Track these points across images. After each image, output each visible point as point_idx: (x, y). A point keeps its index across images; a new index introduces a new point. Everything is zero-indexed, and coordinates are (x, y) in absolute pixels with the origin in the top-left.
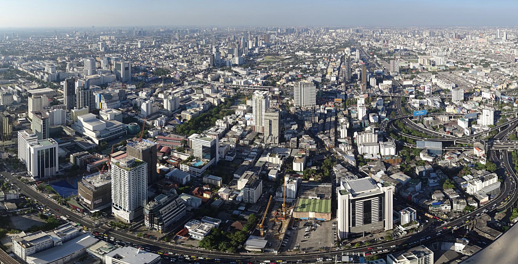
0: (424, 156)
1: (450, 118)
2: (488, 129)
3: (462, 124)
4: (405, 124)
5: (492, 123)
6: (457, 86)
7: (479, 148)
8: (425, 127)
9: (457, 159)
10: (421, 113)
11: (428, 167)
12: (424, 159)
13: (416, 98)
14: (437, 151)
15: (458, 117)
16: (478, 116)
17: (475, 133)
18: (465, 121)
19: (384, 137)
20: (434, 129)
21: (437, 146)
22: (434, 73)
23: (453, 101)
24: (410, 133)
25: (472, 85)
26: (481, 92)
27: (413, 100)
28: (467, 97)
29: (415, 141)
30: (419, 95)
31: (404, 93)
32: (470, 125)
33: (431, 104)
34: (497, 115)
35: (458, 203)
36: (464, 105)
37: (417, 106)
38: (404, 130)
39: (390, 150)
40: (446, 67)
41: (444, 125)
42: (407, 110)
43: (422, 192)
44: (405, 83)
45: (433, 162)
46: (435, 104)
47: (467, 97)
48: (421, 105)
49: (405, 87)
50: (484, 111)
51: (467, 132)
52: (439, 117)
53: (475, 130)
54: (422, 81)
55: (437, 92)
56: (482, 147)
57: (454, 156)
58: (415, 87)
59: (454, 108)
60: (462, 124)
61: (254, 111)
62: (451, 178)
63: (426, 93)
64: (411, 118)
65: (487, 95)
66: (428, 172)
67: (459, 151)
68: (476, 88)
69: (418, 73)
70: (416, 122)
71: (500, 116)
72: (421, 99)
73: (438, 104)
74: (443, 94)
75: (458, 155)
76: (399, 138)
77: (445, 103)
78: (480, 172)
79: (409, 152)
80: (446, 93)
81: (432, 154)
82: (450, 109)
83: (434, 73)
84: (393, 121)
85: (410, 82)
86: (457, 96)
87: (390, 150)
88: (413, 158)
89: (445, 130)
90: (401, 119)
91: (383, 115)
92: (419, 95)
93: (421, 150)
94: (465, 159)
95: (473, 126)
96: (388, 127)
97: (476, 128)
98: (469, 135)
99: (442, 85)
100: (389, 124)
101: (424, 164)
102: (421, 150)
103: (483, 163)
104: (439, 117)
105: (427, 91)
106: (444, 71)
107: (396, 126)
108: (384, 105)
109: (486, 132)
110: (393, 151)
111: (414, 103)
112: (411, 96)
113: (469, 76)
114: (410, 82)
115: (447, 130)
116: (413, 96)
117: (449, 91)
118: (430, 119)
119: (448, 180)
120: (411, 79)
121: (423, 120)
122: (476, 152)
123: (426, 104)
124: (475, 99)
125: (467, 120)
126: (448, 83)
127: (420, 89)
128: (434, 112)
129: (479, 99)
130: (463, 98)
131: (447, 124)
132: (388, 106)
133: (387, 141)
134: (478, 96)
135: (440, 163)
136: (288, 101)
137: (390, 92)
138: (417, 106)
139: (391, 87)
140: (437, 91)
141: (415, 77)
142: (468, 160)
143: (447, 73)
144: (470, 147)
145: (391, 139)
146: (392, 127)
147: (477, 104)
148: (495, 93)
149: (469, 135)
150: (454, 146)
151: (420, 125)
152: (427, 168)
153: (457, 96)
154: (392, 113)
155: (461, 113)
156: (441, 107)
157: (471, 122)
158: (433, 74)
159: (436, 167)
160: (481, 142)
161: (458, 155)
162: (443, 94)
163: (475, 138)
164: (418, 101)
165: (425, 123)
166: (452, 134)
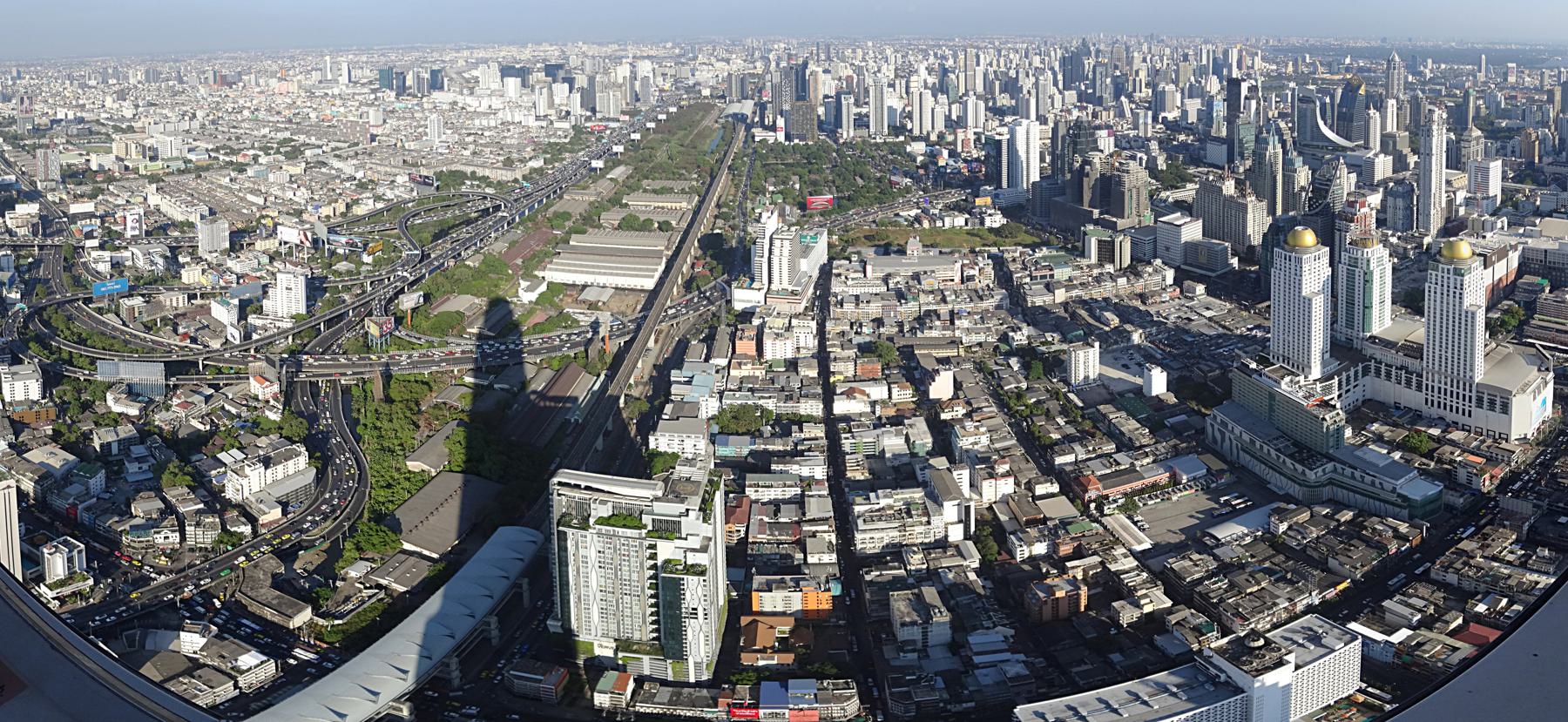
0: (117, 400)
1: (192, 297)
2: (290, 325)
3: (223, 313)
4: (70, 318)
5: (303, 310)
7: (262, 377)
8: (124, 324)
9: (204, 408)
10: (113, 286)
11: (127, 430)
12: (117, 409)
13: (102, 247)
14: (153, 387)
15: (214, 296)
16: (265, 293)
17: (255, 337)
20: (148, 328)
21: (151, 374)
22: (153, 179)
23: (201, 252)
24: (82, 341)
27: (95, 254)
28: (238, 241)
29: (93, 361)
30: (110, 240)
31: (71, 234)
32: (242, 316)
33: (141, 263)
34: (315, 288)
35: (198, 525)
36: (230, 263)
37: (104, 268)
38: (67, 333)
39: (26, 387)
40: (187, 161)
41: (176, 316)
42: (77, 282)
44: (74, 209)
45: (139, 417)
46: (152, 263)
47: (238, 241)
48: (116, 265)
49: (74, 218)
51: (235, 335)
52: (161, 298)
53: (255, 329)
54: (120, 201)
55: (159, 229)
56: (271, 373)
57: (196, 398)
58: (102, 218)
59: (204, 271)
60: (223, 313)
62: (185, 460)
63: (129, 234)
64: (88, 301)
66: (125, 444)
67: (210, 386)
69: (111, 179)
70: (100, 311)
71: (325, 290)
72: (118, 249)
73: (161, 261)
74: (176, 234)
75: (208, 398)
76: (52, 353)
77: (181, 259)
78: (263, 442)
79: (79, 392)
80: (183, 232)
81: (138, 395)
82: (191, 275)
83: (153, 179)
84: (38, 311)
85: (88, 207)
86: (211, 238)
87: (26, 387)
88: (86, 406)
89: (175, 331)
90: (60, 304)
92: (110, 240)
93: (110, 386)
94: (227, 407)
95: (253, 319)
96: (26, 326)
97: (259, 323)
98: (237, 342)
99: (174, 210)
100: (29, 318)
101: (116, 422)
102: (110, 386)
103: (274, 416)
104: (161, 298)
105: (133, 228)
106: (181, 172)
107: (47, 324)
108: (17, 268)
109: (283, 333)
110: (35, 391)
111: (96, 261)
112: (89, 243)
114: (88, 207)
115: (181, 330)
116: (95, 243)
117: (192, 225)
118: (137, 301)
119: (176, 462)
120: (93, 196)
121: (118, 306)
122: (255, 387)
123: (129, 263)
124: (260, 245)
125: (236, 301)
127: (116, 222)
128: (145, 285)
131: (184, 315)
132: (29, 270)
135: (160, 419)
137: (35, 234)
138: (104, 268)
139: (36, 220)
140: (160, 227)
141: (102, 191)
142: (234, 411)
143: (189, 179)
144: (242, 376)
146: (36, 326)
147: (265, 260)
148: (312, 229)
149: (237, 342)
150: (198, 373)
151: (110, 318)
152: (122, 435)
153: (211, 238)
154: (39, 288)
155: (222, 283)
156: (167, 269)
157: (244, 309)
158: (150, 183)
159: (145, 432)
160: (268, 360)
161: (208, 398)
162: (176, 234)
163: (257, 350)
164: (107, 255)
165: (124, 315)
166: (194, 340)
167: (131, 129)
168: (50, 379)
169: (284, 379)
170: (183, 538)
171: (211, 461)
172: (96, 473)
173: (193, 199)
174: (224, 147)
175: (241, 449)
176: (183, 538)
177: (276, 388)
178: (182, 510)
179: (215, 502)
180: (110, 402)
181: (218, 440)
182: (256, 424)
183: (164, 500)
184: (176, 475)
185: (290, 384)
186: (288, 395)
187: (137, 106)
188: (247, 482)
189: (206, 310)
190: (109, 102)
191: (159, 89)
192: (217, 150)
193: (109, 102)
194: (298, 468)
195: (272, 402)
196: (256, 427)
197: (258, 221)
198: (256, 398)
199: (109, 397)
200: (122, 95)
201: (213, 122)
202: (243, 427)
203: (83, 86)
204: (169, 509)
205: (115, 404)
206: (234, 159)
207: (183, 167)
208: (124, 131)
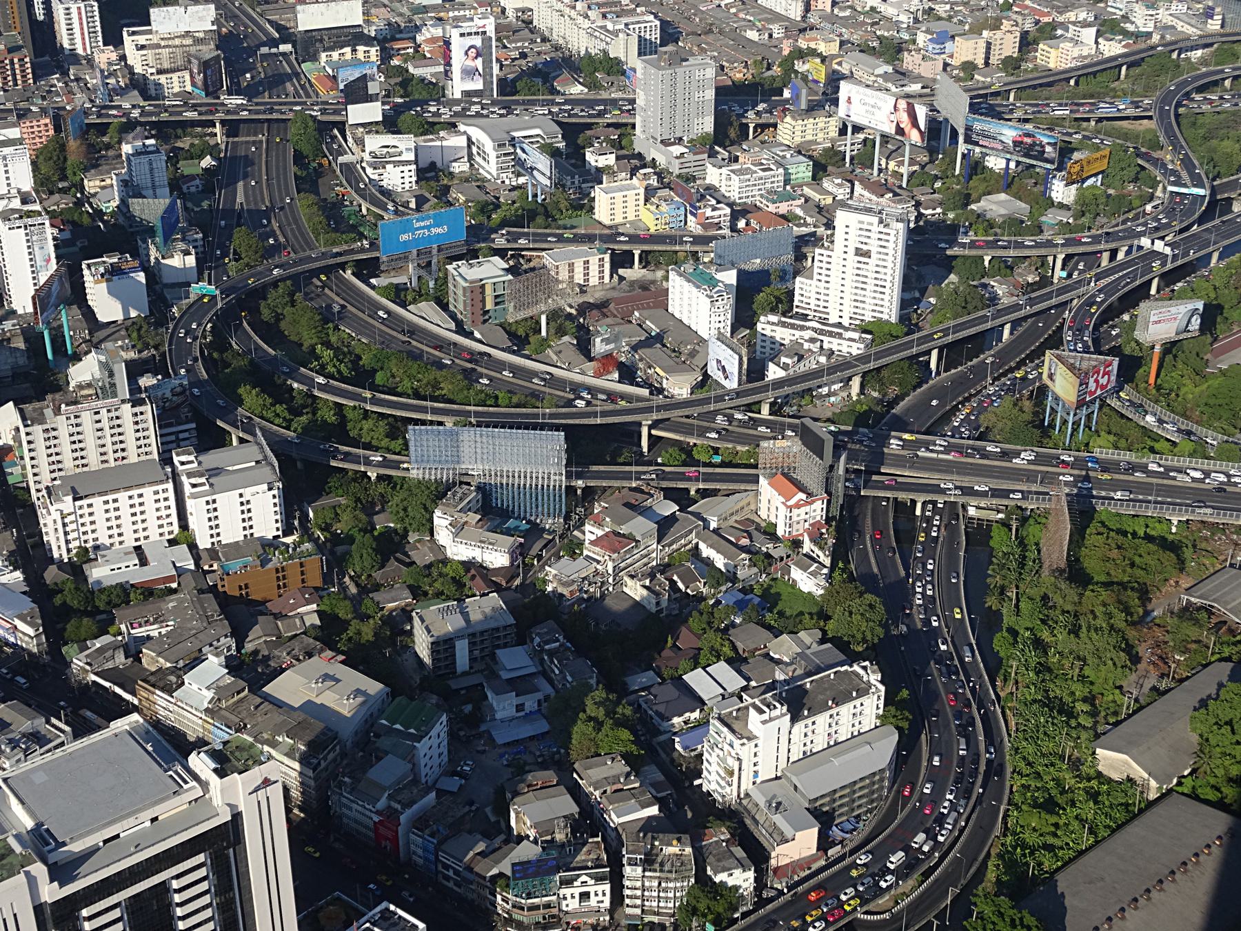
2: (856, 349)
4: (327, 317)
5: (890, 313)
6: (669, 34)
7: (790, 480)
8: (460, 329)
9: (656, 552)
10: (430, 228)
11: (484, 606)
12: (459, 551)
13: (390, 124)
14: (538, 493)
15: (674, 260)
16: (800, 257)
17: (774, 372)
18: (712, 283)
19: (197, 416)
20: (519, 339)
21: (530, 460)
23: (641, 141)
24: (362, 377)
25: (778, 32)
26: (834, 80)
27: (374, 143)
30: (413, 106)
32: (744, 317)
33: (491, 167)
36: (714, 175)
37: (399, 179)
38: (327, 354)
42: (336, 218)
43: (454, 784)
45: (509, 573)
46: (521, 167)
48: (431, 173)
50: (842, 218)
51: (726, 364)
52: (547, 259)
53: (775, 350)
56: (810, 469)
57: (640, 526)
58: (387, 41)
62: (616, 687)
63: (458, 87)
64: (368, 269)
65: (870, 106)
67: (670, 494)
68: (801, 54)
70: (399, 294)
72: (429, 128)
73: (543, 163)
74: (577, 90)
75: (665, 525)
76: (296, 412)
77: (590, 157)
79: (369, 509)
80: (593, 85)
81: (505, 514)
84: (244, 303)
86: (668, 104)
88: (390, 546)
89: (584, 347)
90: (300, 281)
91: (176, 261)
92: (413, 106)
93: (440, 492)
94: (706, 551)
95: (768, 326)
96: (219, 343)
97: (784, 335)
100: (225, 322)
101: (459, 584)
102: (440, 492)
104: (547, 259)
105: (469, 73)
107: (271, 332)
109: (840, 368)
111: (379, 162)
112: (359, 113)
117: (615, 68)
118: (491, 269)
119: (600, 694)
122: (771, 504)
123: (460, 167)
129: (819, 131)
131: (601, 307)
133: (220, 440)
134: (813, 108)
135: (557, 576)
138: (399, 179)
140: (535, 72)
142: (720, 562)
144: (743, 472)
145: (249, 428)
146: (248, 341)
149: (732, 384)
150: (640, 460)
151: (425, 315)
152: (475, 616)
153: (668, 104)
154: (240, 238)
156: (559, 185)
159: (531, 608)
161: (665, 525)
162: (577, 90)
163: (776, 409)
164: (405, 144)
166: (628, 374)
169: (839, 488)
170: (618, 897)
171: (669, 691)
175: (737, 662)
176: (618, 897)
177: (817, 510)
178: (615, 819)
179: (686, 807)
180: (443, 536)
181: (686, 640)
182: (770, 598)
183: (576, 792)
184: (599, 725)
185: (852, 503)
186: (844, 526)
188: (754, 754)
189: (656, 297)
194: (859, 719)
196: (771, 607)
197: (788, 68)
198: (770, 532)
199: (441, 521)
202: (740, 606)
204: (588, 820)
205: (455, 540)
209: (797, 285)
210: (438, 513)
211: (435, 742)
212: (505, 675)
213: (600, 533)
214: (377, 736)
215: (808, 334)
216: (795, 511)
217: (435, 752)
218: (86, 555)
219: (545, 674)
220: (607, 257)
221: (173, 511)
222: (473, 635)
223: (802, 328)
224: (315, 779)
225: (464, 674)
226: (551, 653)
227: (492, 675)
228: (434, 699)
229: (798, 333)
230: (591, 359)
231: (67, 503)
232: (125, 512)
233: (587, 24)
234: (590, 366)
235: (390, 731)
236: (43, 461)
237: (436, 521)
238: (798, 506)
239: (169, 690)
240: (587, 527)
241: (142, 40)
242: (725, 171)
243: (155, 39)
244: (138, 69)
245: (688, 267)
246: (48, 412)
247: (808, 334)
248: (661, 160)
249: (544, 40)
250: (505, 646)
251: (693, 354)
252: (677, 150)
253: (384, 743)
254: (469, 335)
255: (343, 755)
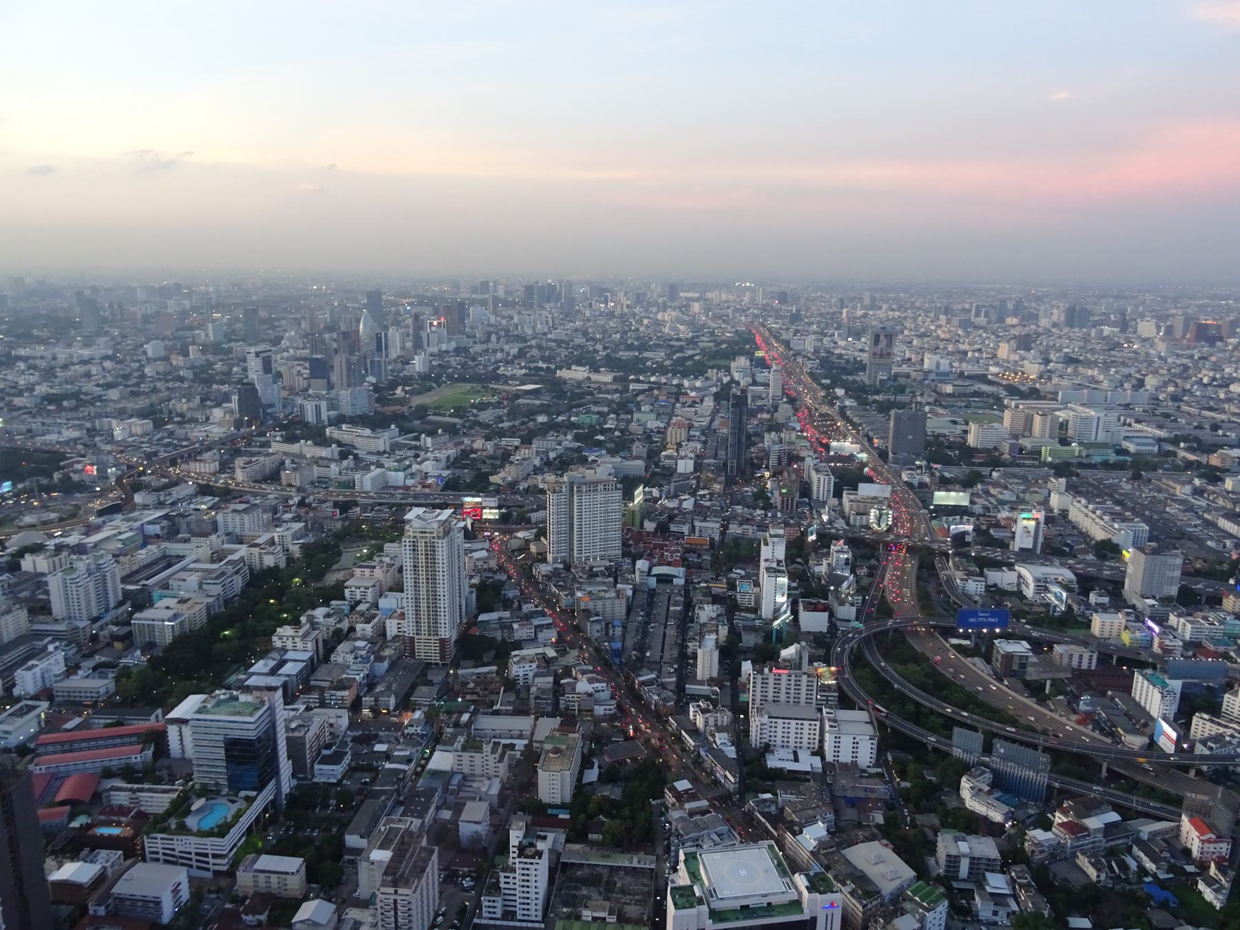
12: (974, 805)
18: (1164, 685)
60: (1150, 695)
61: (408, 583)
66: (979, 867)
99: (1092, 522)
106: (1106, 465)
113: (1221, 502)
115: (1082, 707)
122: (1191, 836)
125: (1176, 685)
126: (1116, 516)
130: (1174, 591)
136: (527, 542)
158: (1058, 475)
167: (1034, 394)
168: (888, 740)
172: (936, 902)
173: (1124, 509)
174: (1185, 439)
180: (966, 793)
187: (1047, 361)
190: (1004, 351)
191: (1086, 339)
192: (1175, 441)
193: (1004, 351)
195: (1213, 871)
199: (965, 783)
200: (1025, 343)
201: (1175, 398)
203: (965, 324)
206: (1203, 459)
207: (1113, 458)
208: (1023, 396)
209: (1225, 699)
210: (964, 779)
211: (938, 916)
212: (989, 889)
213: (1065, 820)
214: (904, 900)
215: (1229, 732)
216: (1206, 845)
217: (937, 922)
218: (767, 748)
219: (1015, 897)
220: (1095, 656)
221: (817, 737)
222: (973, 858)
223: (1226, 727)
224: (863, 913)
225: (963, 880)
226: (1021, 886)
227: (981, 887)
228: (942, 890)
229: (1222, 730)
230: (1075, 712)
231: (765, 719)
232: (793, 731)
233: (1102, 523)
234: (1074, 717)
235: (911, 900)
236: (758, 694)
237: (963, 784)
238: (1209, 841)
239: (794, 834)
240: (1057, 814)
241: (852, 497)
242: (1182, 620)
243: (858, 498)
244: (847, 510)
245: (1149, 671)
246: (766, 670)
247: (1229, 732)
248: (1139, 605)
249: (1074, 527)
250: (992, 871)
251: (1145, 725)
252: (1150, 602)
253: (908, 906)
254: (1000, 680)
255: (882, 905)
